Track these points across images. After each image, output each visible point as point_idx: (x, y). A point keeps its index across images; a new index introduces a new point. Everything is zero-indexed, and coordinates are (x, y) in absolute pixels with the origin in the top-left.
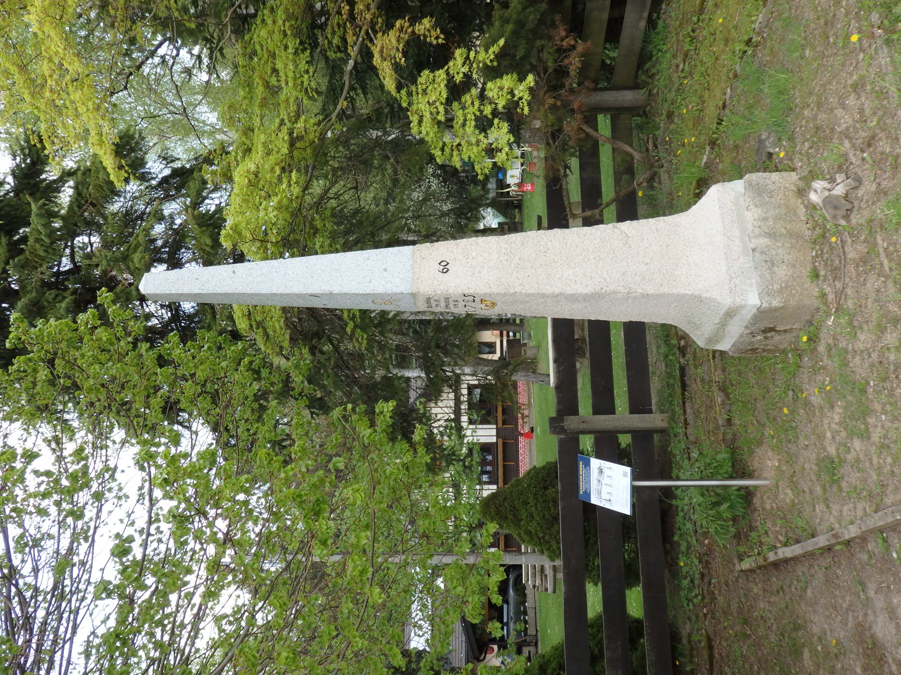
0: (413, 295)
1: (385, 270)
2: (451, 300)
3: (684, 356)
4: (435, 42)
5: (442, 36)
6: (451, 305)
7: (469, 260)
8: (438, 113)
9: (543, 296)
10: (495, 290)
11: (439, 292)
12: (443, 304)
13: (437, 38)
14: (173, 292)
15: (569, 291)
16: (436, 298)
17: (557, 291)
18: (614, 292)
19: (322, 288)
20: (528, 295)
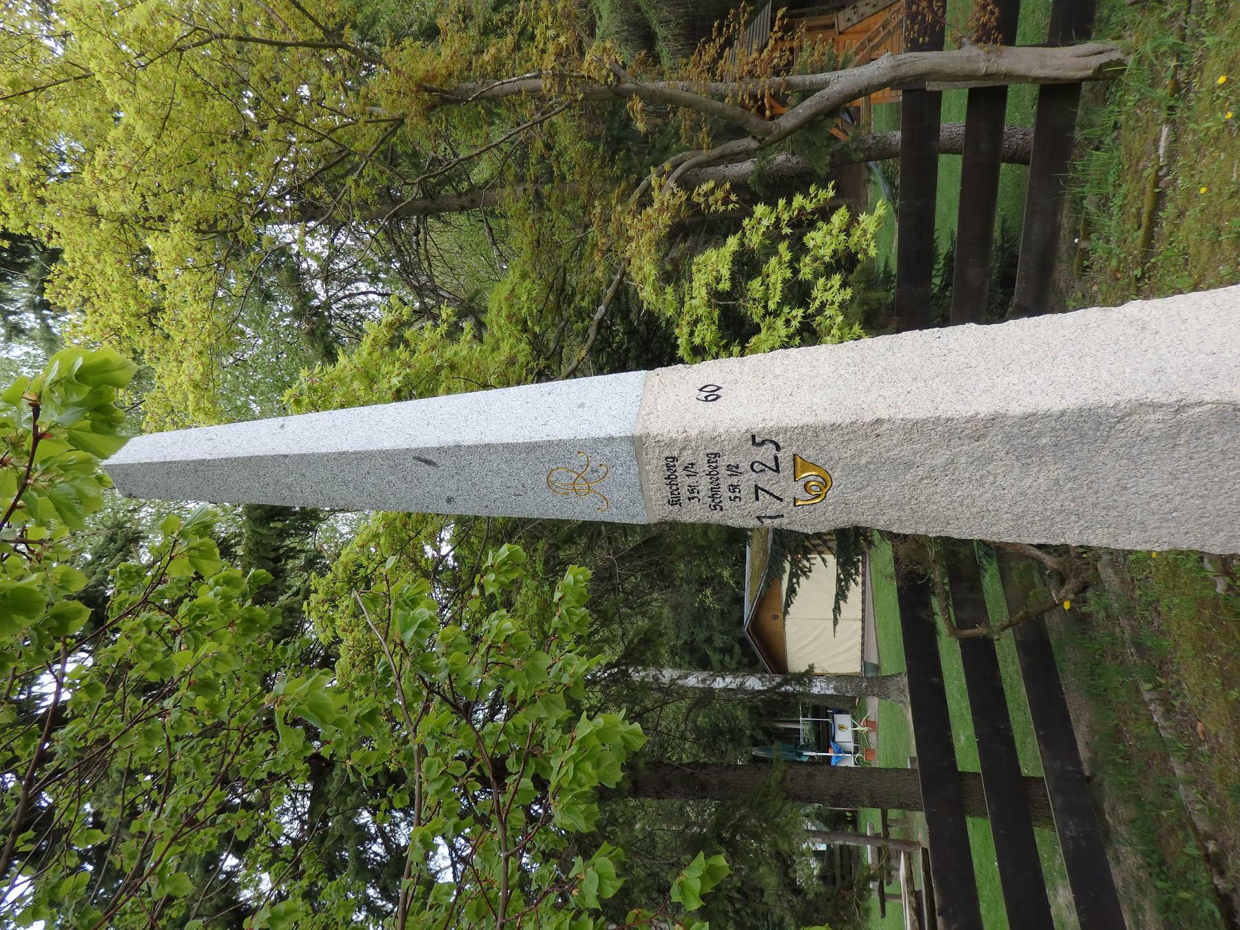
0: (637, 443)
1: (582, 406)
2: (723, 462)
3: (1222, 873)
4: (722, 208)
5: (733, 197)
6: (724, 492)
7: (766, 380)
8: (718, 280)
9: (947, 431)
10: (827, 418)
11: (693, 433)
12: (704, 484)
13: (726, 201)
14: (155, 460)
15: (1016, 409)
16: (687, 457)
17: (984, 407)
18: (1142, 406)
19: (442, 439)
20: (914, 429)
